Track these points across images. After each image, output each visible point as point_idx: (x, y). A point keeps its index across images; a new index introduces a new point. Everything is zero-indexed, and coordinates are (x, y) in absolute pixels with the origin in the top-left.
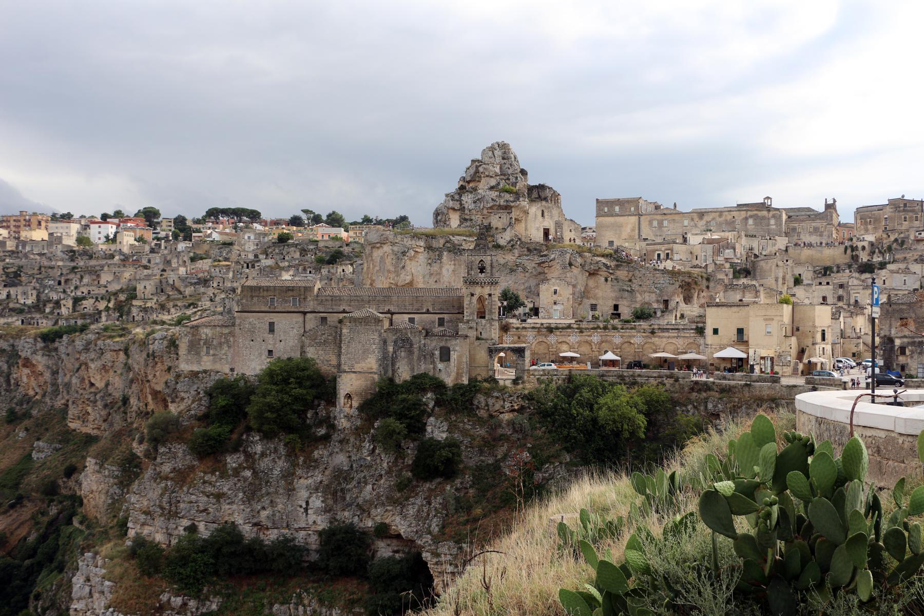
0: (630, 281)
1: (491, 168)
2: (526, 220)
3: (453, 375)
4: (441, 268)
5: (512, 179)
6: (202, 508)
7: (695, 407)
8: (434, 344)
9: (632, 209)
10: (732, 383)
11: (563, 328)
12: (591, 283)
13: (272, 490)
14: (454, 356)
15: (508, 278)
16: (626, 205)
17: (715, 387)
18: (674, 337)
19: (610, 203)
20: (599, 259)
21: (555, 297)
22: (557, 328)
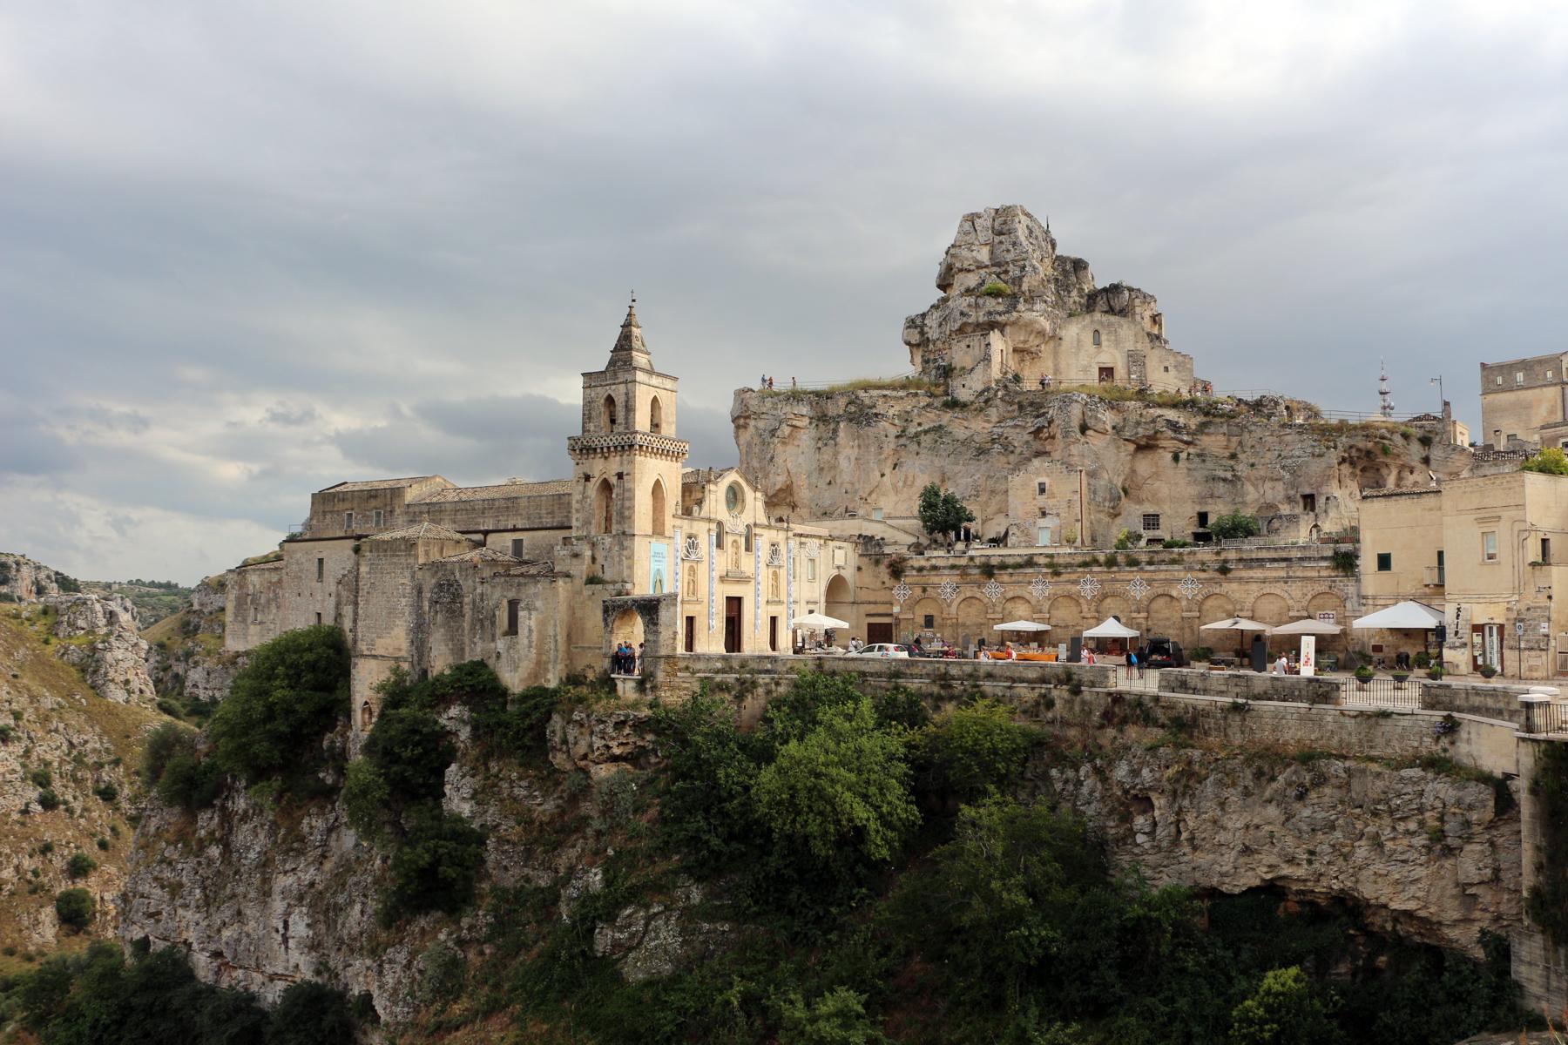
0: (1233, 456)
1: (965, 253)
2: (1056, 354)
3: (526, 666)
4: (836, 455)
5: (1014, 271)
6: (152, 910)
7: (1098, 771)
8: (498, 596)
9: (1549, 374)
10: (1201, 700)
11: (1019, 566)
12: (1144, 465)
13: (241, 889)
14: (527, 621)
15: (972, 469)
16: (1537, 368)
17: (1159, 713)
18: (1277, 580)
19: (1507, 369)
20: (1159, 411)
21: (1042, 500)
22: (1003, 567)
